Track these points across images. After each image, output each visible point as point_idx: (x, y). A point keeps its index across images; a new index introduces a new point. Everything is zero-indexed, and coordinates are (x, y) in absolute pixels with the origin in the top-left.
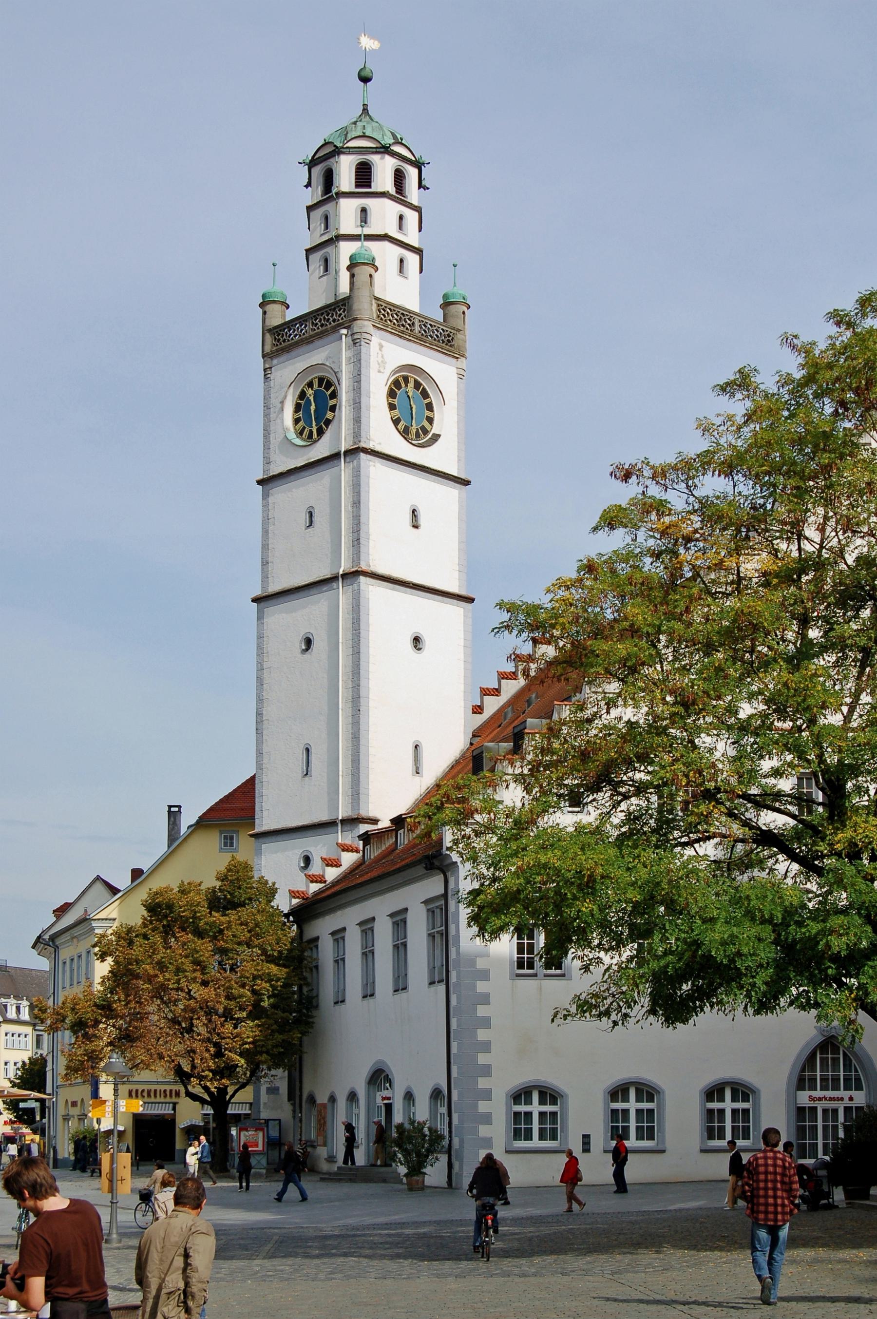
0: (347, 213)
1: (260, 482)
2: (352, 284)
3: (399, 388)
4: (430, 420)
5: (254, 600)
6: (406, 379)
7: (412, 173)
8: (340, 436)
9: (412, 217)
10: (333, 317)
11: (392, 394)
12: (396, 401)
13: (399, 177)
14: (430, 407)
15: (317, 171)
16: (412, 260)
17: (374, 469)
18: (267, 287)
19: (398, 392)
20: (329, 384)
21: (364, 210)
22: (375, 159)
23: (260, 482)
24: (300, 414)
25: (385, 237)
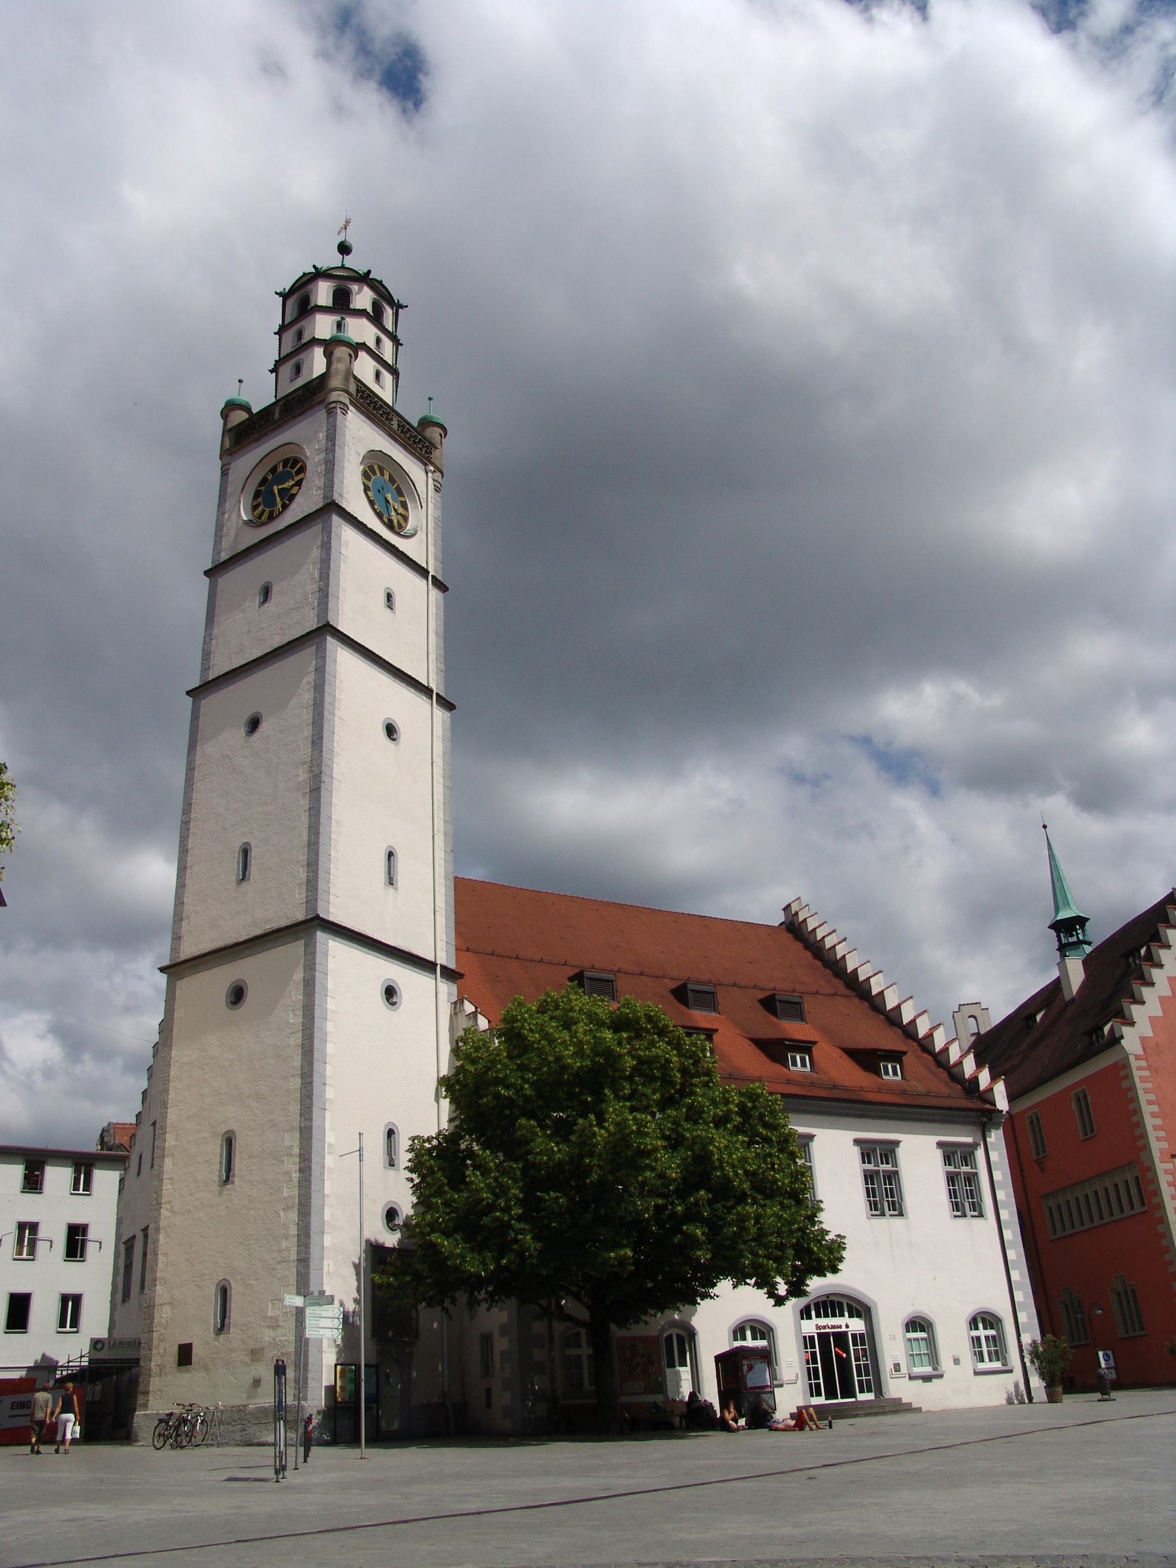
0: (323, 326)
1: (207, 573)
2: (329, 364)
3: (375, 474)
4: (406, 519)
5: (188, 693)
6: (381, 470)
7: (389, 313)
8: (305, 502)
9: (388, 344)
10: (304, 400)
11: (366, 475)
12: (370, 484)
13: (376, 306)
14: (404, 505)
15: (291, 302)
16: (387, 377)
17: (347, 535)
18: (232, 394)
19: (373, 478)
20: (296, 461)
21: (339, 326)
22: (355, 287)
23: (207, 573)
24: (260, 500)
25: (363, 346)
